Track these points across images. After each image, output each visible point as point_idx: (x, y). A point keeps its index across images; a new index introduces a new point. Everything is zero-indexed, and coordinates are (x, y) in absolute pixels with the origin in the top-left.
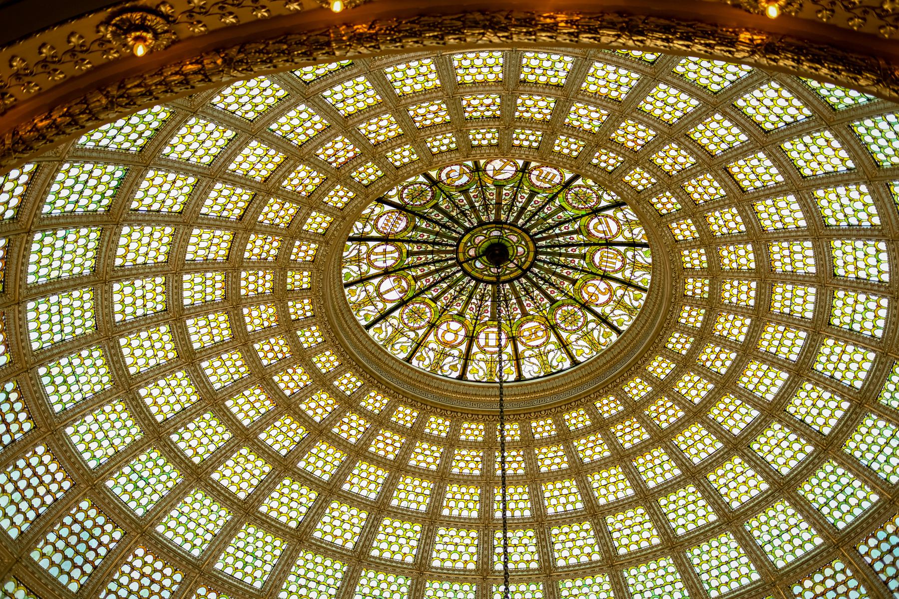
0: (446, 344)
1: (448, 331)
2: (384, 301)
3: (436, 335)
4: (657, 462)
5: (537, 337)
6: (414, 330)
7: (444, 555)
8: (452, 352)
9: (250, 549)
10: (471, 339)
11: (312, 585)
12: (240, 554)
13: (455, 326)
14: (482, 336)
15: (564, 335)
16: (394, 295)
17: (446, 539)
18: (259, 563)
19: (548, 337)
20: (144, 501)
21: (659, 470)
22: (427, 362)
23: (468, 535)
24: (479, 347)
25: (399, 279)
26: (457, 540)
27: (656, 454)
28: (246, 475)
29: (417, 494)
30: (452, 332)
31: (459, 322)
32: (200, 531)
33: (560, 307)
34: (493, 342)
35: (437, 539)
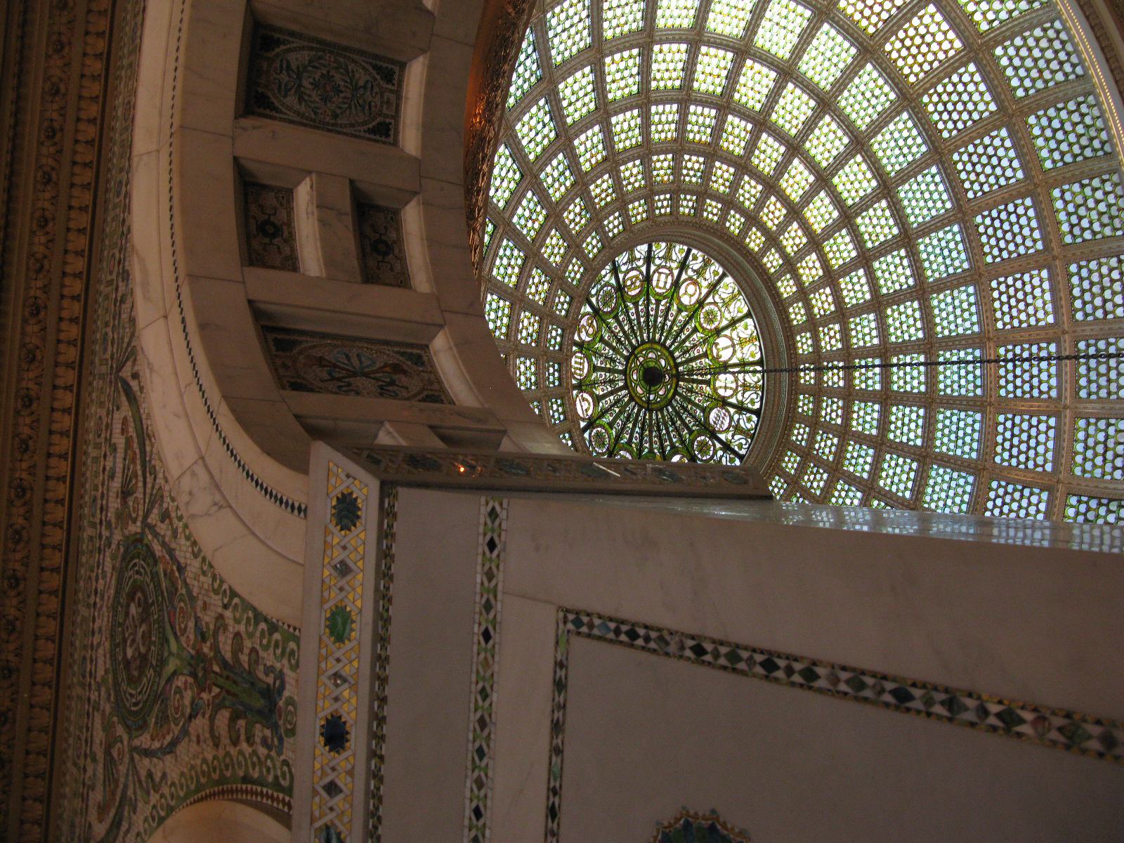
0: (696, 283)
1: (691, 296)
2: (731, 339)
5: (631, 279)
6: (715, 303)
9: (897, 151)
10: (676, 284)
11: (868, 95)
12: (905, 150)
13: (686, 300)
14: (668, 286)
16: (723, 342)
17: (758, 97)
18: (896, 135)
20: (949, 236)
25: (719, 357)
28: (875, 221)
29: (764, 152)
31: (680, 303)
32: (923, 187)
34: (663, 277)
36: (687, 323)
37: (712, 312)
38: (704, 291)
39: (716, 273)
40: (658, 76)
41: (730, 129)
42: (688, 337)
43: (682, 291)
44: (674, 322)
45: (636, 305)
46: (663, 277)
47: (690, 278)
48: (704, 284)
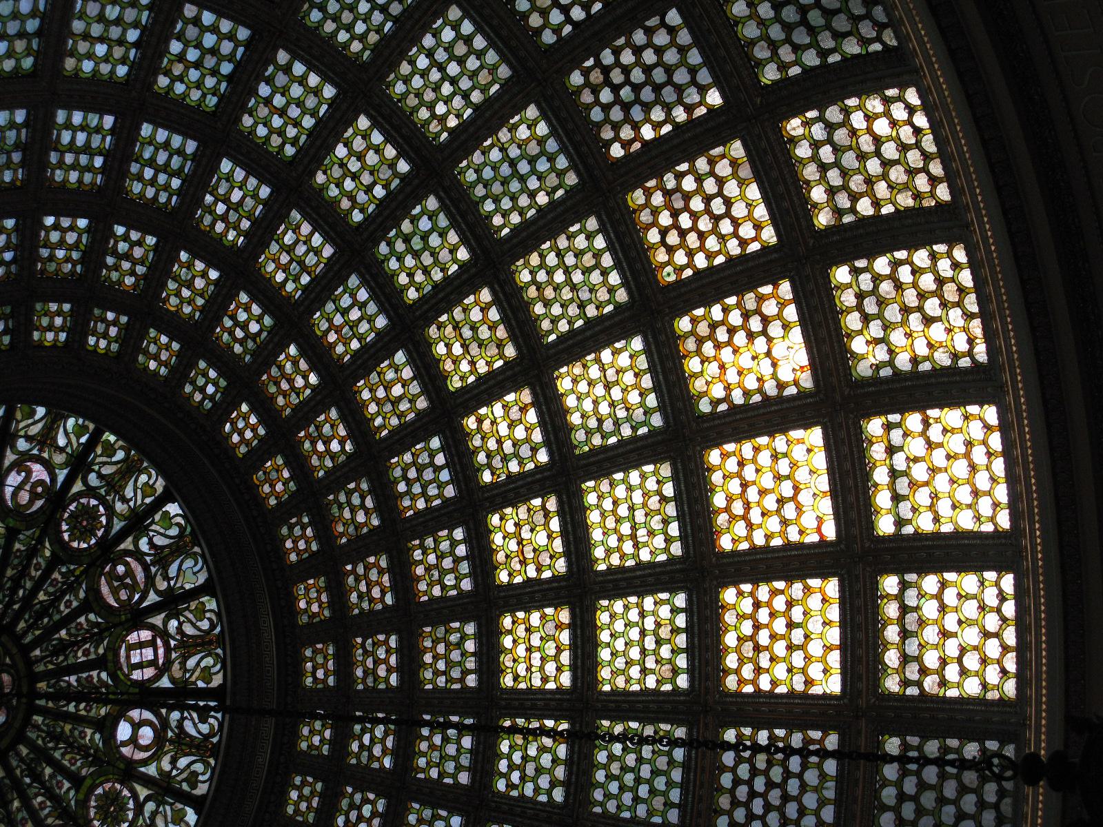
0: (159, 739)
1: (133, 740)
3: (145, 762)
4: (338, 320)
5: (130, 573)
7: (550, 668)
8: (173, 724)
10: (147, 696)
13: (124, 731)
14: (136, 675)
15: (118, 525)
19: (127, 553)
21: (355, 314)
22: (199, 767)
23: (510, 632)
24: (157, 677)
26: (521, 651)
27: (324, 325)
30: (133, 732)
33: (65, 546)
34: (148, 654)
35: (523, 686)
36: (83, 750)
37: (123, 808)
38: (151, 770)
39: (193, 779)
40: (486, 425)
41: (454, 638)
42: (59, 768)
43: (135, 714)
44: (76, 719)
45: (85, 608)
46: (148, 654)
47: (165, 723)
48: (166, 765)
